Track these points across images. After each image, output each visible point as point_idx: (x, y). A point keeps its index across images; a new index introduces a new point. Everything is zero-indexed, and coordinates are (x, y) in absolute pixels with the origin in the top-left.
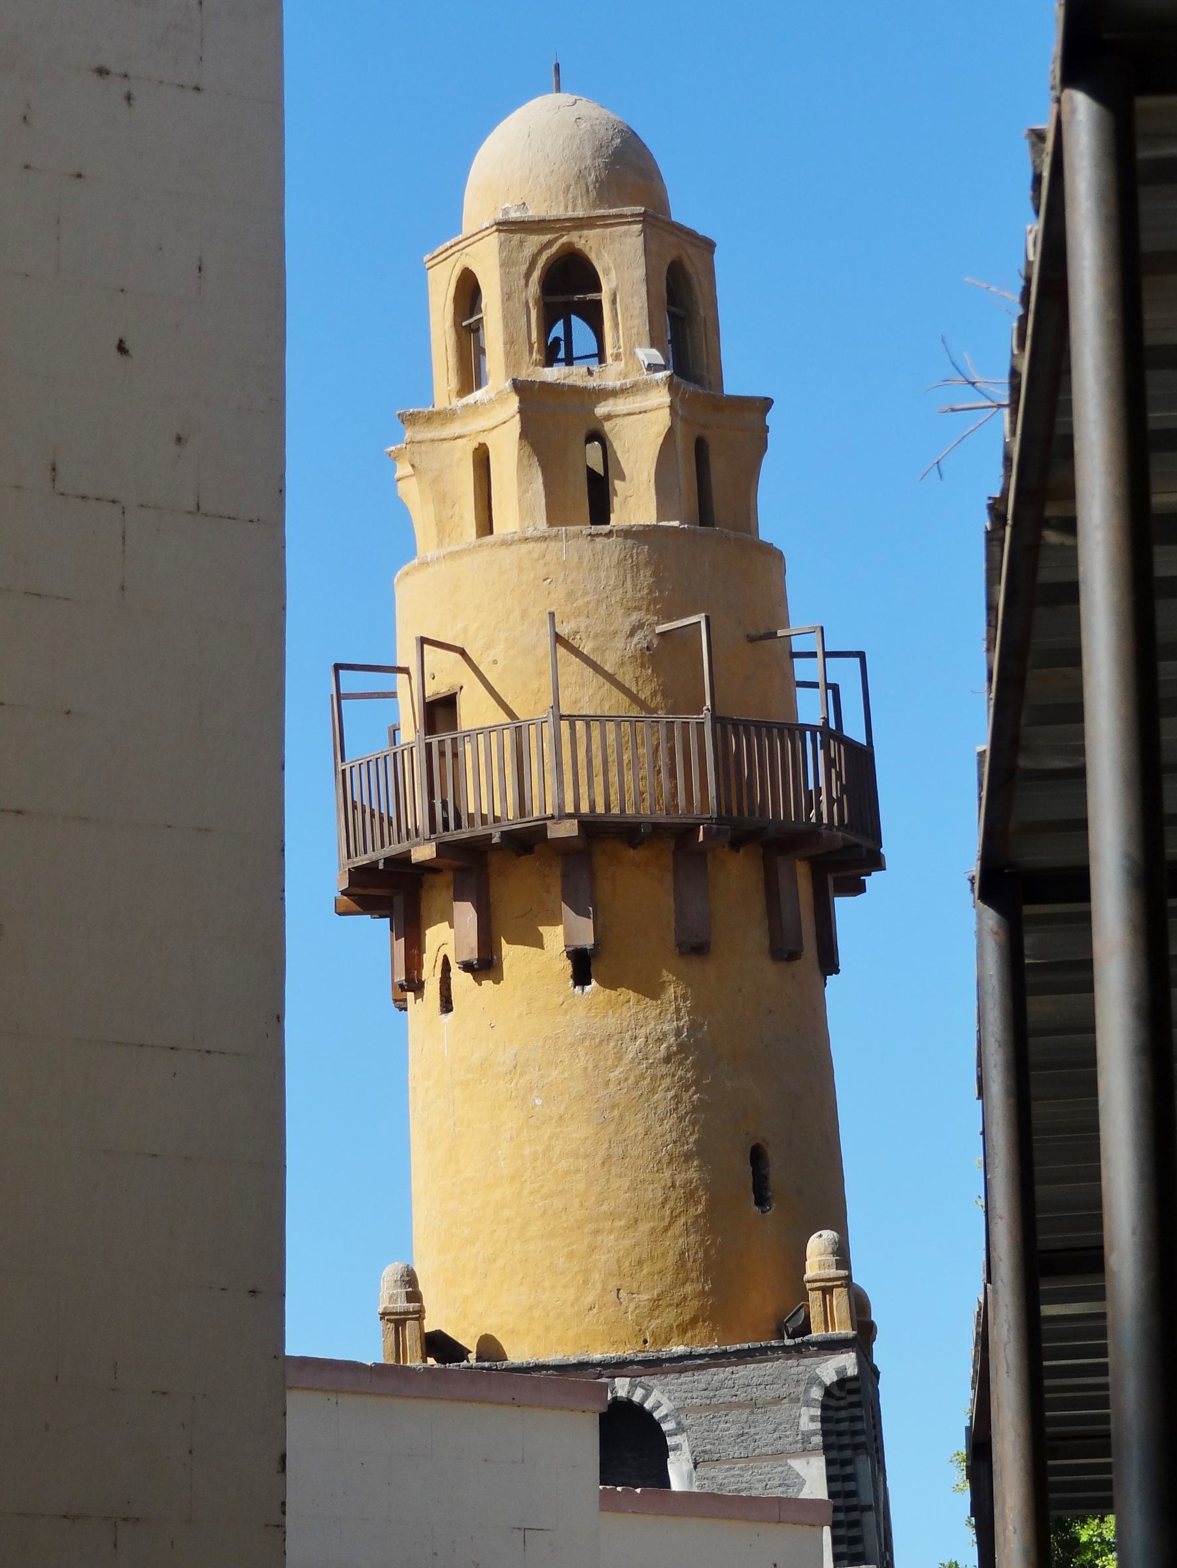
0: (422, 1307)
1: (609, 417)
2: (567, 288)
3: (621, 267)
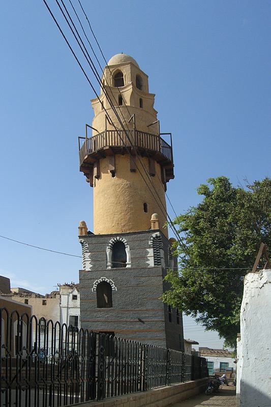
0: (236, 351)
1: (122, 92)
2: (118, 79)
3: (126, 72)
